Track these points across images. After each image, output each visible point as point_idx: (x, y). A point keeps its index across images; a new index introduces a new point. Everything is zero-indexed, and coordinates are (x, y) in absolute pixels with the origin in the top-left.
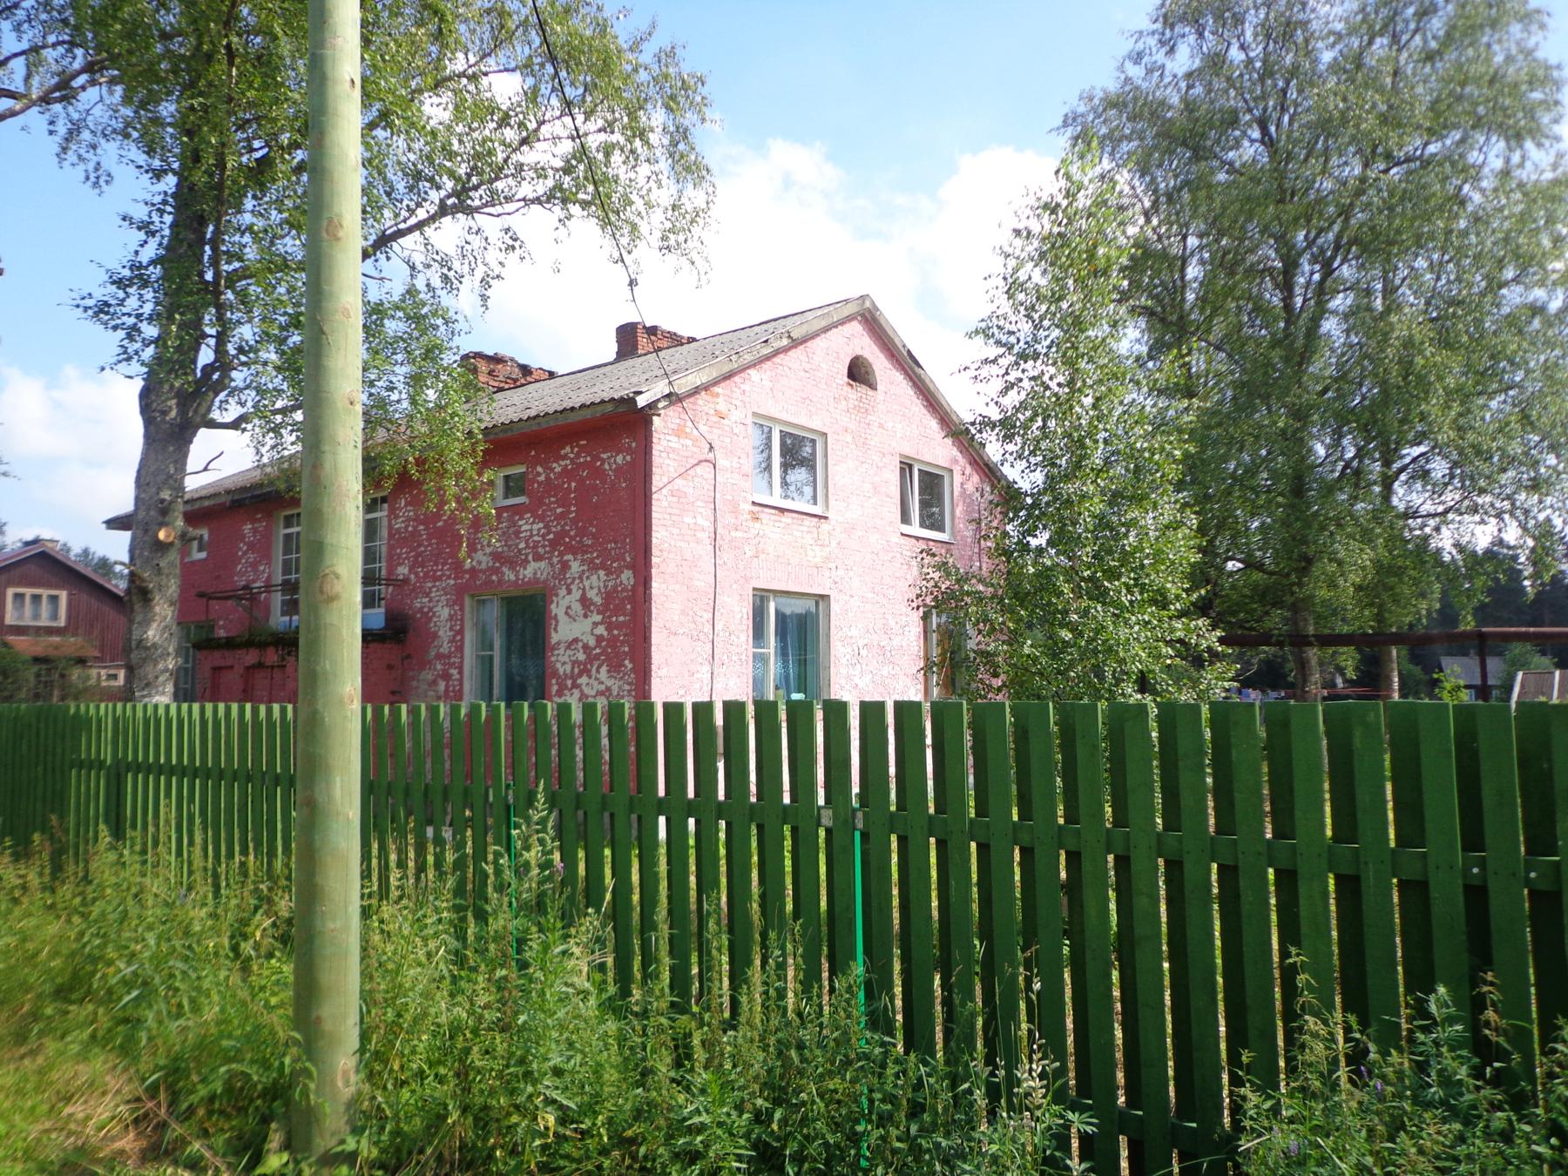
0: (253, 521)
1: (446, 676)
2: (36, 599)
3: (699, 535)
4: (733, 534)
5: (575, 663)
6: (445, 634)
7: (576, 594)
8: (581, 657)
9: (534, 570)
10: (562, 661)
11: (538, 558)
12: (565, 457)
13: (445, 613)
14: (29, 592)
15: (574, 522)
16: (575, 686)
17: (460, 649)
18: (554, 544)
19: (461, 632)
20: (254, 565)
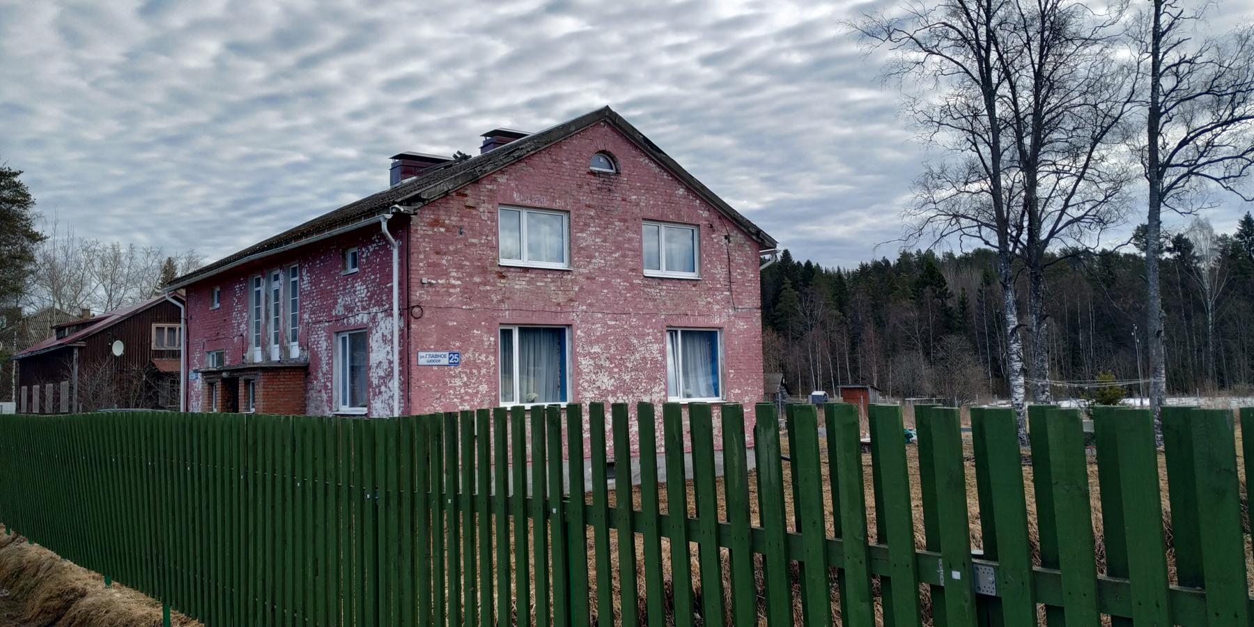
0: (240, 282)
1: (326, 387)
2: (160, 329)
3: (452, 290)
4: (482, 288)
5: (380, 377)
6: (324, 359)
7: (380, 334)
8: (382, 374)
9: (363, 318)
10: (375, 376)
11: (364, 308)
12: (374, 242)
13: (324, 345)
14: (166, 326)
15: (379, 284)
16: (380, 393)
17: (331, 368)
18: (370, 298)
19: (331, 358)
20: (241, 312)
